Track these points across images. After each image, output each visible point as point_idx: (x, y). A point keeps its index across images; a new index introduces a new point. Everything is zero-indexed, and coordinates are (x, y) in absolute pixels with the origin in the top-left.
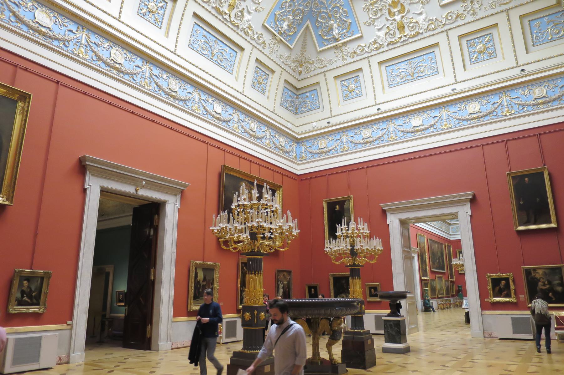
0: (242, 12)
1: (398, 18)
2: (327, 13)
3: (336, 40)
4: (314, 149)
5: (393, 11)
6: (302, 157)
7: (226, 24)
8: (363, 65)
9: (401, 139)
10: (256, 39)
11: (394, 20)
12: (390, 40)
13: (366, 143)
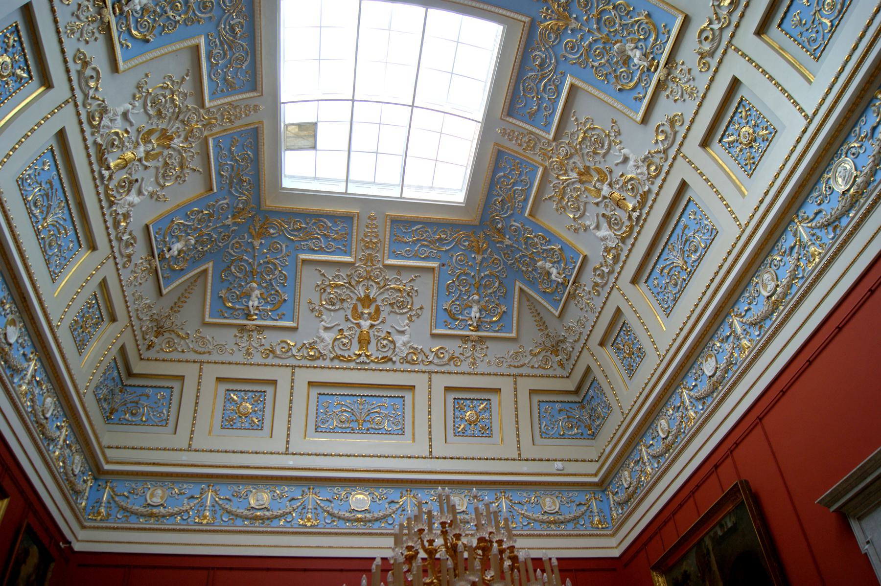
0: (131, 183)
1: (365, 324)
7: (96, 187)
8: (282, 376)
11: (359, 325)
12: (339, 352)
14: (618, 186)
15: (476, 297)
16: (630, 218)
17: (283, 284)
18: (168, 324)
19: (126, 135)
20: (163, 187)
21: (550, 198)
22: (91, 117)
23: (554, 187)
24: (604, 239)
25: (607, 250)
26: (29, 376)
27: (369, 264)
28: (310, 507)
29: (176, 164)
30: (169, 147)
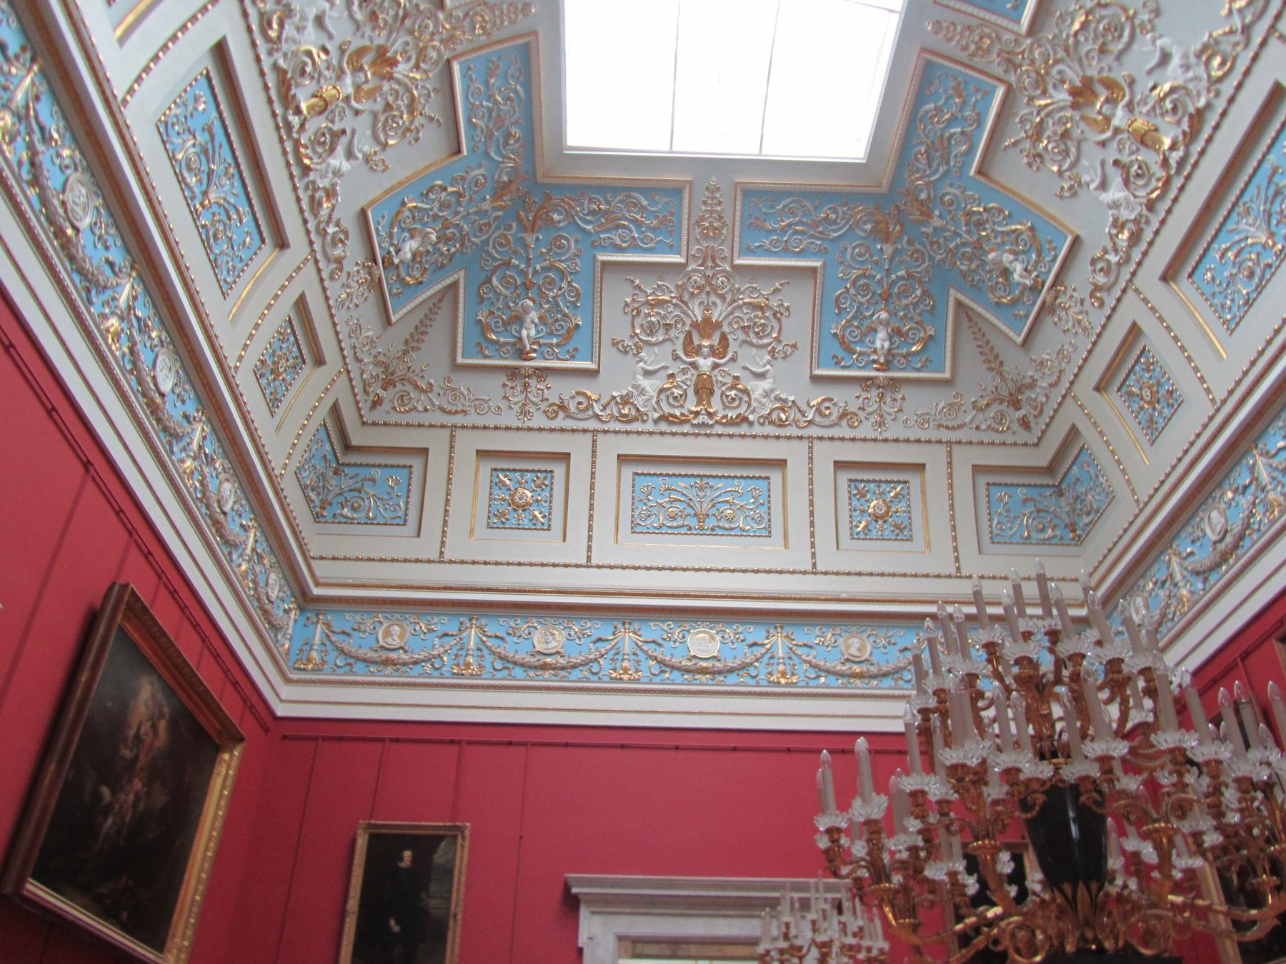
2: (523, 273)
3: (522, 354)
4: (359, 644)
5: (696, 342)
6: (309, 660)
7: (281, 141)
8: (578, 448)
9: (651, 682)
10: (329, 239)
12: (667, 410)
13: (545, 667)
14: (1145, 110)
15: (884, 315)
16: (1165, 163)
17: (574, 303)
18: (400, 370)
19: (323, 56)
20: (385, 146)
21: (1015, 144)
22: (265, 23)
23: (1021, 121)
24: (1115, 205)
25: (1119, 225)
26: (195, 446)
27: (710, 264)
28: (627, 650)
29: (403, 109)
30: (390, 77)
